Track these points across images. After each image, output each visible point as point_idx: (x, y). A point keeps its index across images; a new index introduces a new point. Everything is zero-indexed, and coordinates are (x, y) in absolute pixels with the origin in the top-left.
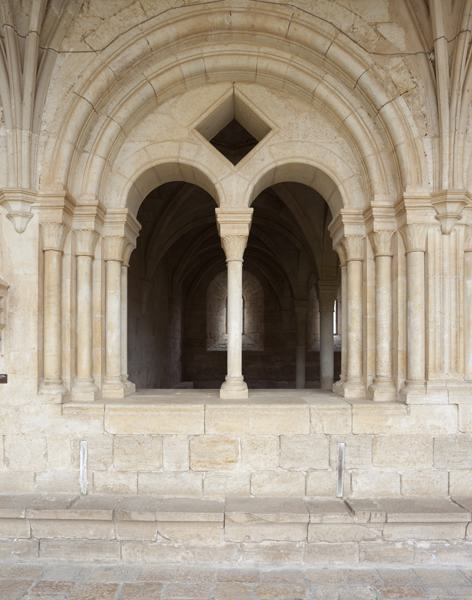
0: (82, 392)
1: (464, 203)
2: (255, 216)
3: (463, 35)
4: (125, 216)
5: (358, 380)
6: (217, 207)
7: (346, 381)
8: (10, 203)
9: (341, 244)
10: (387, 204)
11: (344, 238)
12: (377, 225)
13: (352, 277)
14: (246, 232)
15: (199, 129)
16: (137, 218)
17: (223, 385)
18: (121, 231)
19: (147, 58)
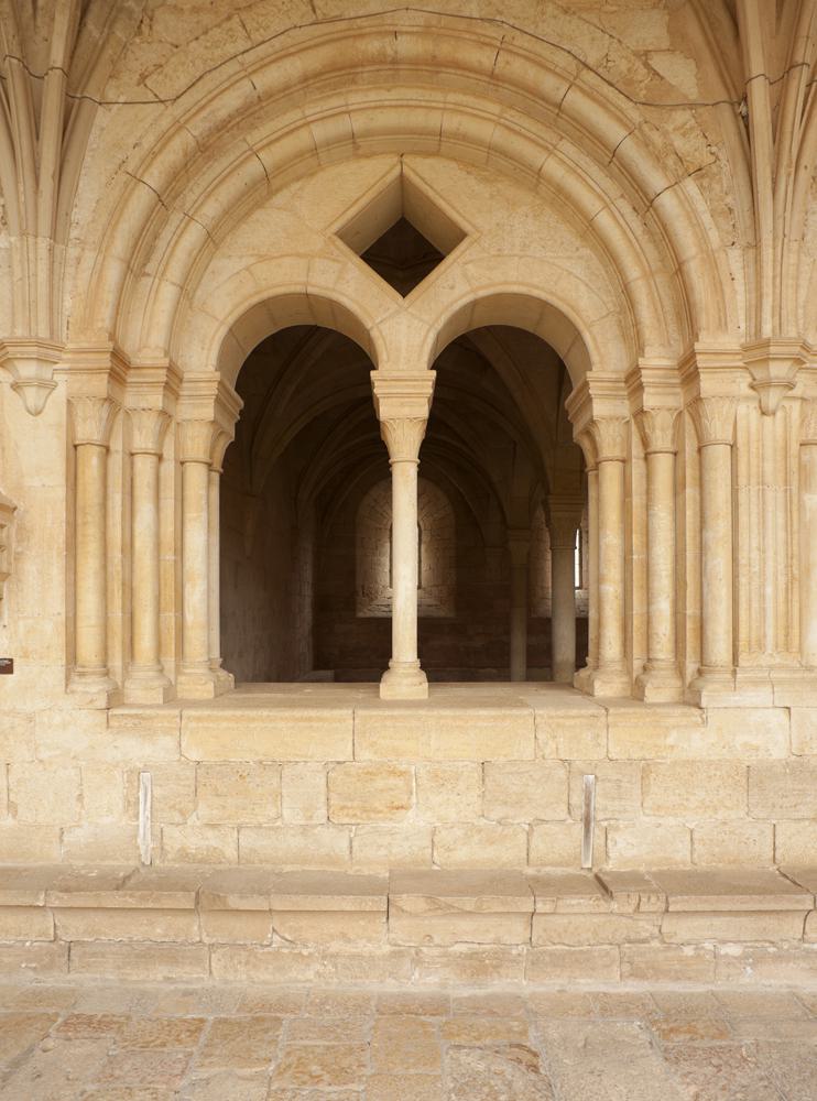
0: (142, 689)
1: (799, 361)
2: (438, 384)
3: (796, 72)
4: (216, 385)
5: (618, 667)
6: (374, 369)
7: (597, 668)
8: (16, 362)
9: (588, 433)
10: (665, 363)
11: (592, 422)
12: (650, 400)
13: (607, 489)
14: (423, 411)
15: (342, 235)
16: (236, 390)
17: (386, 676)
18: (209, 412)
19: (250, 113)
